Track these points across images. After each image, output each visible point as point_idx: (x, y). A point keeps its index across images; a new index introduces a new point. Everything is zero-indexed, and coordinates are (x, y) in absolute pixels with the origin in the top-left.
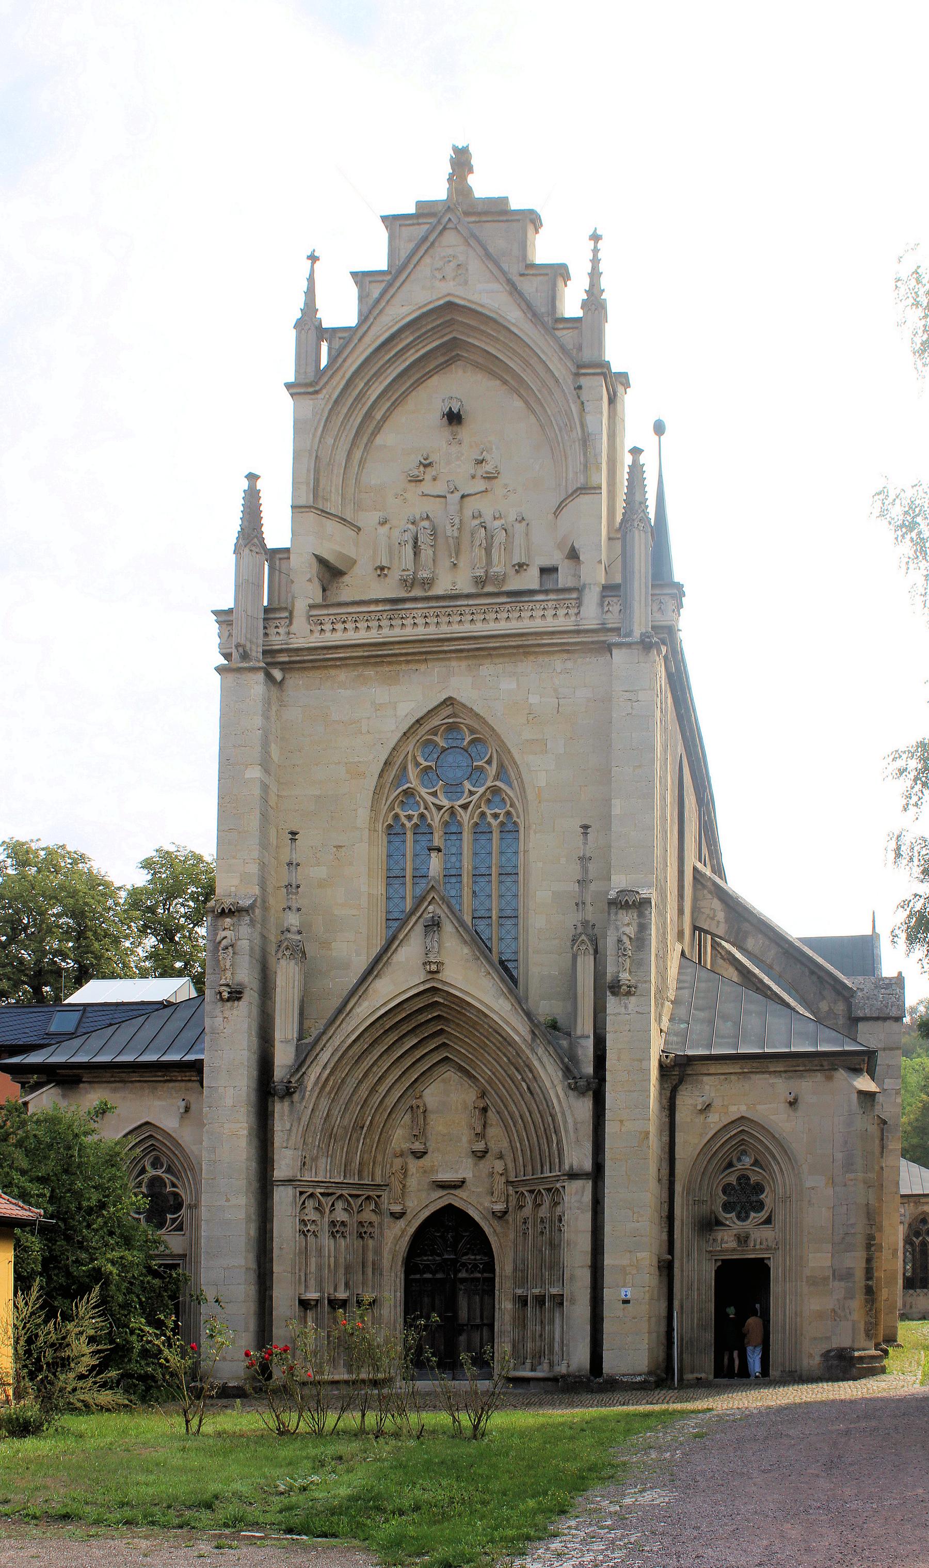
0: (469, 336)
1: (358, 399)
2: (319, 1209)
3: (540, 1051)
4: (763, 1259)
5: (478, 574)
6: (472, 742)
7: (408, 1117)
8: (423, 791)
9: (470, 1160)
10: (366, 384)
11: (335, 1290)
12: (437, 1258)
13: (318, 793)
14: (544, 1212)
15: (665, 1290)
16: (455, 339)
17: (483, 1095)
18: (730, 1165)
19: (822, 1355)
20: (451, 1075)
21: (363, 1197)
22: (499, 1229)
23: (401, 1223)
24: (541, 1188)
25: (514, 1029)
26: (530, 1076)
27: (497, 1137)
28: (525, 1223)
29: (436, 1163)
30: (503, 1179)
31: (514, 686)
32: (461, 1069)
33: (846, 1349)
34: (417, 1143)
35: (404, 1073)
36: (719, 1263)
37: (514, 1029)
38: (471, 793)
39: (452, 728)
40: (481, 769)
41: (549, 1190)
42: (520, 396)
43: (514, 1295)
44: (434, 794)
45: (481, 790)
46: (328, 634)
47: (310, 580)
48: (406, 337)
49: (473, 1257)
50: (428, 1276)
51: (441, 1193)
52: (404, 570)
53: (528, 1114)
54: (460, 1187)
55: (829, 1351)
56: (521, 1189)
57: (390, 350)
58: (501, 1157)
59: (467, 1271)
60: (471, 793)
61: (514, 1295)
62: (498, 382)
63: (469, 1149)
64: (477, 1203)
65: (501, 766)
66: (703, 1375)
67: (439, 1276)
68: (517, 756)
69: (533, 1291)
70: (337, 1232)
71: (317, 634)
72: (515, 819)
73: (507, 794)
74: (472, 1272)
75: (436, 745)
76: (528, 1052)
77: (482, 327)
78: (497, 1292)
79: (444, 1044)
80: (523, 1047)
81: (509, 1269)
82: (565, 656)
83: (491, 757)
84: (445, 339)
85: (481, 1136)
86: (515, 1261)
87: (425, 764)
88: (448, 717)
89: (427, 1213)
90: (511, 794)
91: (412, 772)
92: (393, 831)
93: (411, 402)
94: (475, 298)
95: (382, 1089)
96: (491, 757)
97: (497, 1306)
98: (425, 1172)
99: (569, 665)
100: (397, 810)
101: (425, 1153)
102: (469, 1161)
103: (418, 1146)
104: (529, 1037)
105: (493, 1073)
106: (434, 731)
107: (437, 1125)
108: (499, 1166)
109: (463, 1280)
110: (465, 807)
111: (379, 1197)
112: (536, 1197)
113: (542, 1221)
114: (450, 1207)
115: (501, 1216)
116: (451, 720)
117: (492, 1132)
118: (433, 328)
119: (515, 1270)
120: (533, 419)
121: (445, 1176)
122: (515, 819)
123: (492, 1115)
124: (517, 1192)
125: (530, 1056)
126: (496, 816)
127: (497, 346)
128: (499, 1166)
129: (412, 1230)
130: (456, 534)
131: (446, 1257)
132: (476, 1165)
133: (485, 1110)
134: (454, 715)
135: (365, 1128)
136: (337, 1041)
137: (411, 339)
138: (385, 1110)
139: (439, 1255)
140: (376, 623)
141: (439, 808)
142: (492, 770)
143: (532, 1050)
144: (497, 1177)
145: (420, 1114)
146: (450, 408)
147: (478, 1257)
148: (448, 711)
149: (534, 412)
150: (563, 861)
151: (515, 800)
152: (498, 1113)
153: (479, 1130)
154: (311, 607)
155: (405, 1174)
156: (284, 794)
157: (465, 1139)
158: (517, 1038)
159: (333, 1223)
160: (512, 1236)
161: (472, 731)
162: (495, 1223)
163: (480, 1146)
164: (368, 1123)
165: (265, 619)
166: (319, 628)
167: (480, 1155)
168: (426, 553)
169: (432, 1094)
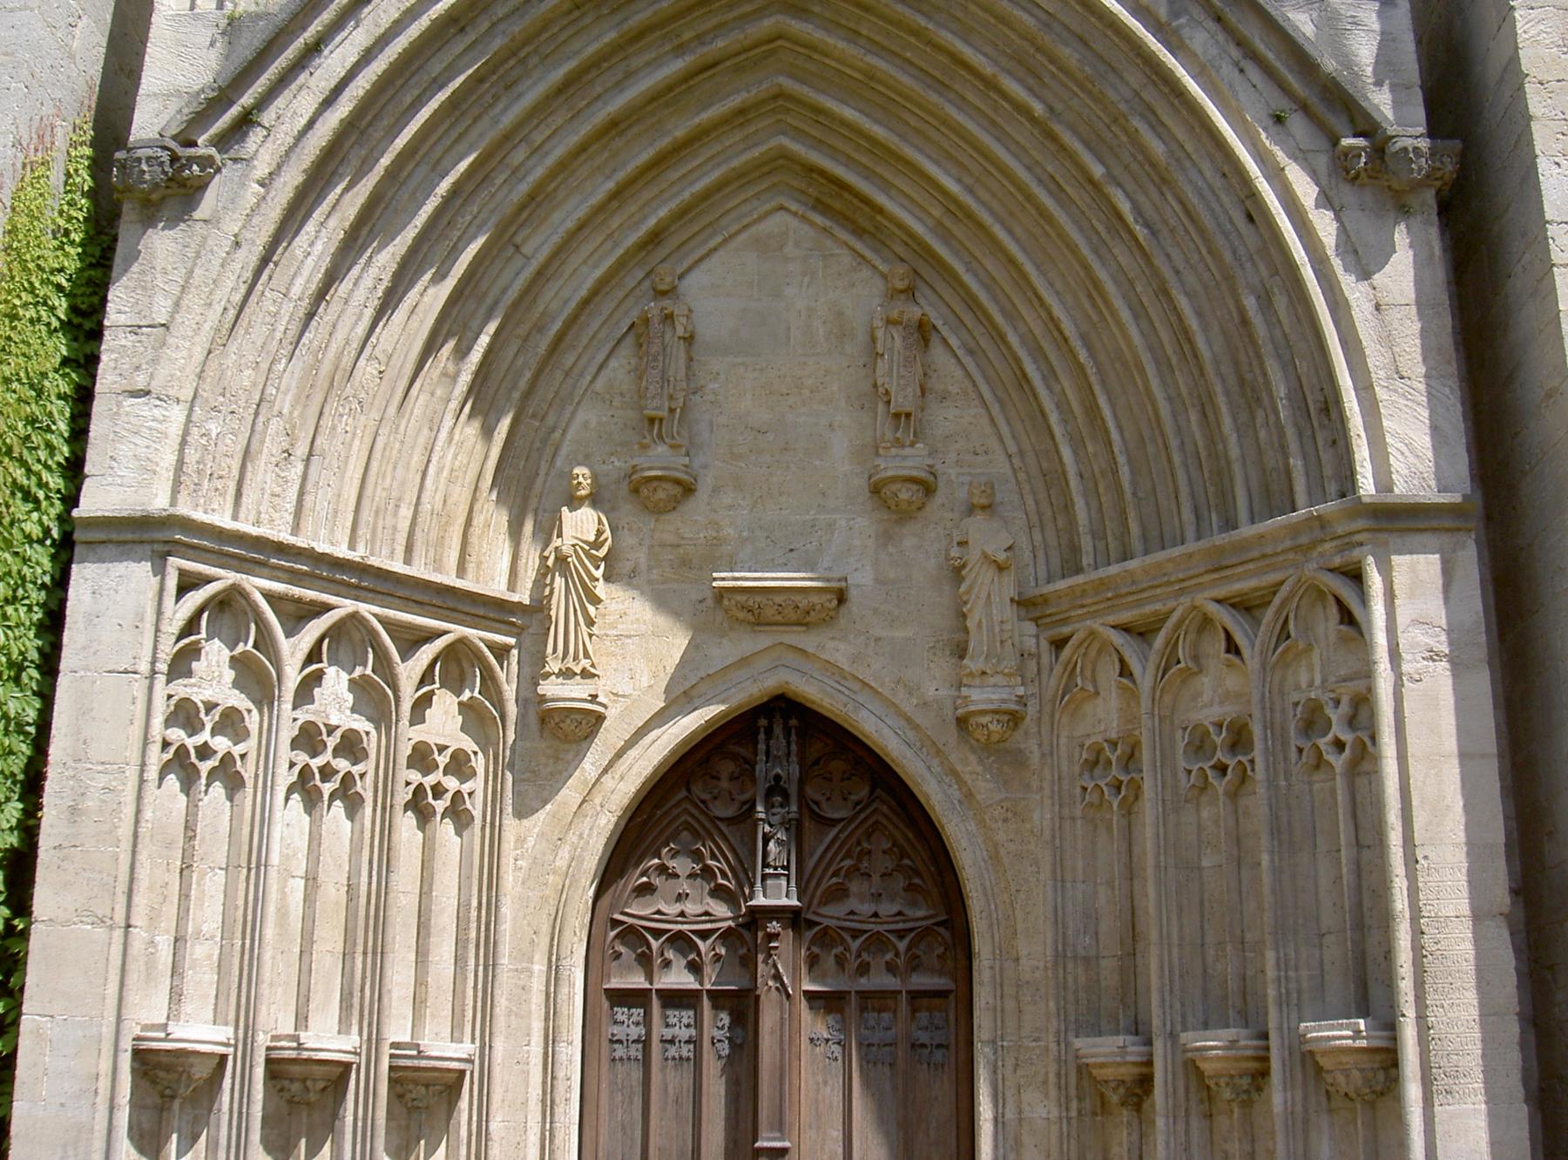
2: (255, 678)
7: (620, 368)
9: (862, 522)
11: (302, 1019)
20: (788, 224)
21: (440, 644)
22: (984, 788)
27: (966, 434)
29: (729, 531)
30: (1007, 588)
34: (661, 449)
35: (616, 195)
49: (866, 908)
51: (749, 643)
54: (828, 620)
56: (1095, 624)
59: (840, 962)
63: (860, 483)
70: (327, 772)
74: (864, 969)
79: (780, 95)
81: (1034, 952)
86: (1058, 921)
95: (539, 244)
98: (685, 562)
101: (688, 490)
107: (734, 396)
108: (987, 538)
111: (501, 652)
115: (996, 740)
117: (947, 418)
119: (1060, 957)
131: (760, 900)
132: (886, 538)
138: (540, 328)
144: (981, 580)
147: (887, 908)
153: (904, 399)
157: (840, 445)
159: (308, 738)
160: (1042, 816)
162: (970, 766)
167: (898, 500)
169: (715, 291)
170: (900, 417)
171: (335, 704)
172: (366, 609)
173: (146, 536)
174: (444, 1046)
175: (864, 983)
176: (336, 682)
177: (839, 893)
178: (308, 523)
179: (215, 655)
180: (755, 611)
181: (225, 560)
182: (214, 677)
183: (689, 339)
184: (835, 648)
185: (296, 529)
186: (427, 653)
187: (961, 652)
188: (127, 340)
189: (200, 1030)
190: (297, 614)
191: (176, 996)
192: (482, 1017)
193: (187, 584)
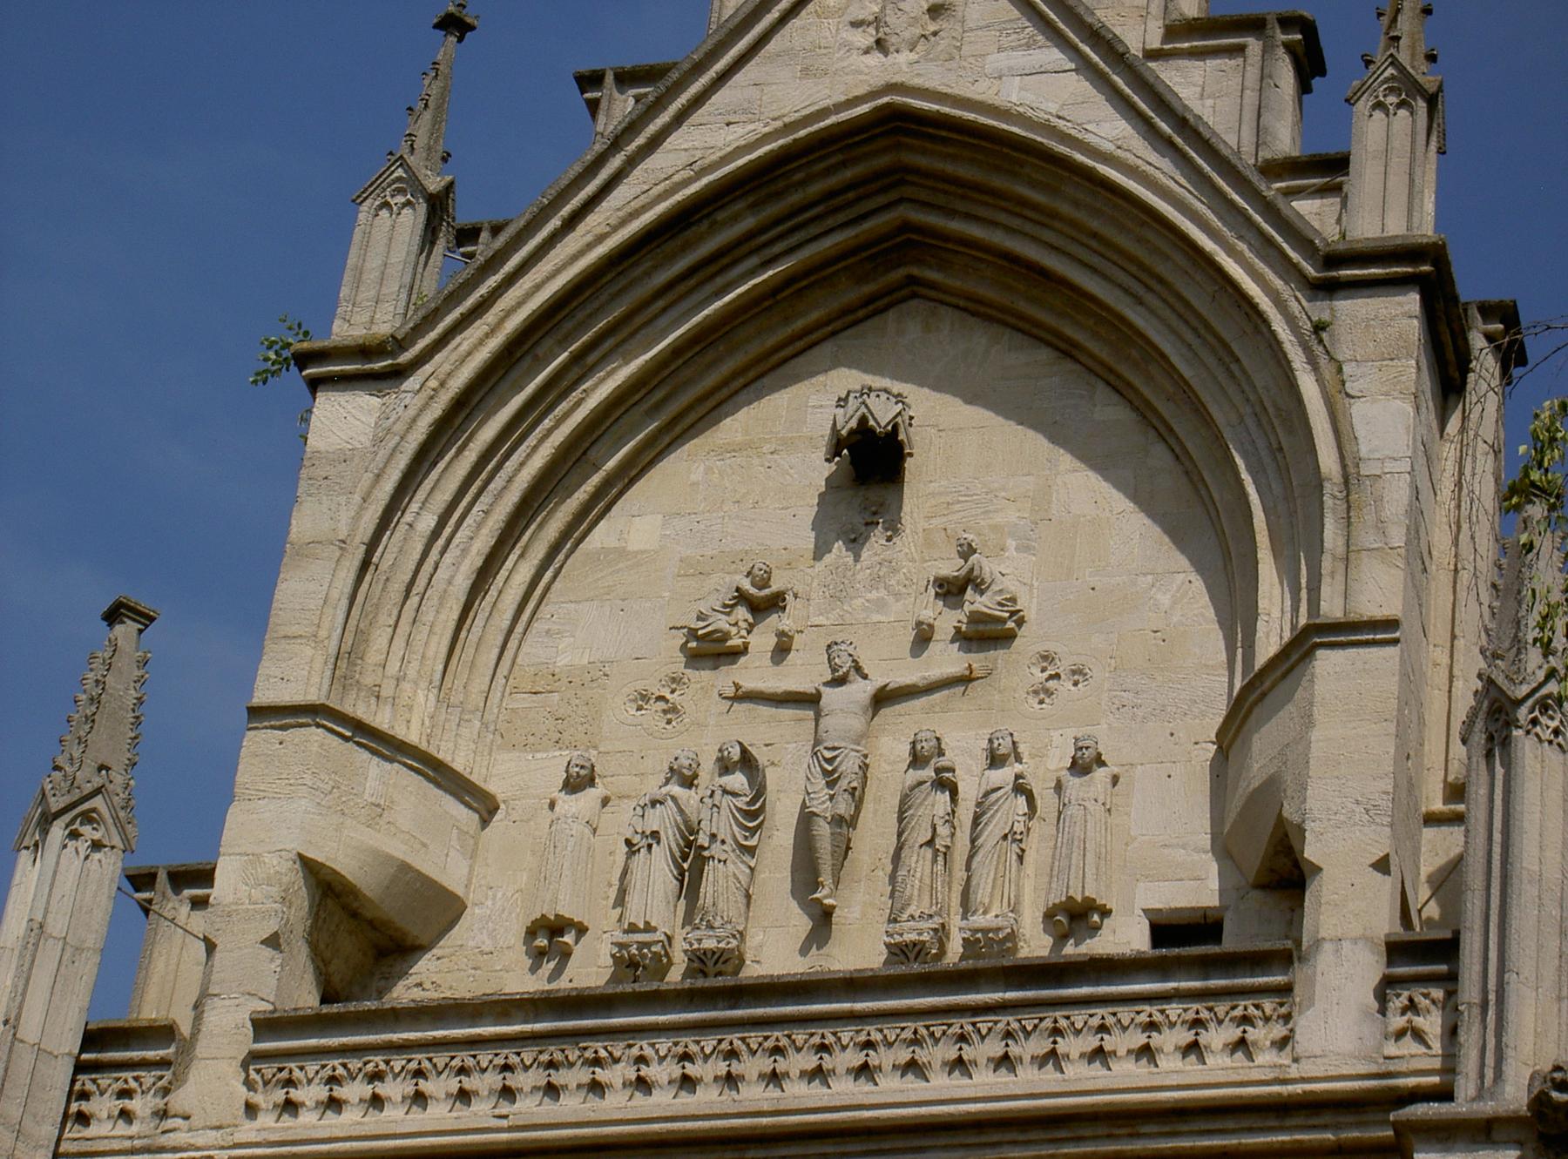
0: (952, 213)
5: (911, 937)
10: (576, 358)
16: (906, 227)
42: (1121, 389)
46: (307, 1118)
47: (273, 942)
48: (735, 219)
52: (633, 929)
57: (671, 258)
62: (1044, 354)
71: (266, 1120)
77: (998, 182)
93: (735, 426)
94: (982, 91)
118: (831, 194)
120: (1160, 456)
127: (1047, 235)
130: (844, 807)
137: (749, 223)
140: (493, 1080)
146: (863, 420)
149: (1163, 432)
154: (264, 1026)
165: (81, 1068)
166: (279, 1095)
168: (720, 881)
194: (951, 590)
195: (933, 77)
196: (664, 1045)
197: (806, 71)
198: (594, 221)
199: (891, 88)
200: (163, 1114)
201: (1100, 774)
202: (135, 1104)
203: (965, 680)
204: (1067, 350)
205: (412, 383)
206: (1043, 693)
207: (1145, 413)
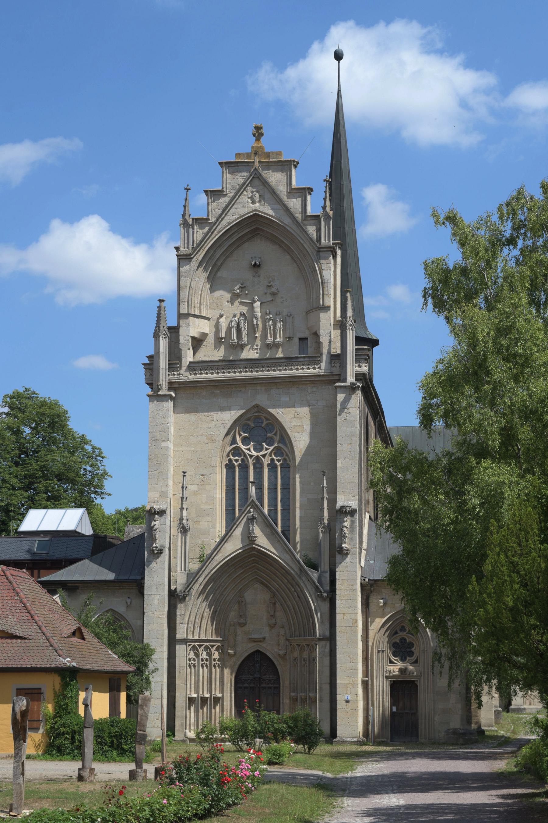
1: (210, 258)
3: (304, 578)
4: (414, 681)
6: (267, 424)
7: (236, 607)
8: (243, 447)
11: (203, 692)
12: (251, 677)
13: (193, 449)
14: (305, 655)
15: (365, 695)
17: (274, 596)
18: (396, 633)
19: (445, 732)
20: (258, 585)
23: (234, 659)
24: (304, 644)
25: (291, 568)
26: (299, 589)
28: (295, 660)
30: (285, 638)
31: (287, 399)
32: (262, 583)
33: (457, 729)
36: (392, 682)
37: (291, 568)
38: (267, 449)
39: (257, 418)
40: (271, 438)
41: (308, 645)
43: (290, 696)
44: (249, 449)
45: (272, 448)
50: (246, 685)
51: (253, 644)
53: (297, 607)
55: (449, 730)
58: (283, 627)
60: (267, 449)
61: (290, 696)
64: (271, 649)
65: (281, 436)
66: (385, 740)
67: (252, 685)
68: (289, 433)
69: (301, 694)
70: (204, 663)
72: (288, 462)
73: (284, 450)
74: (268, 684)
75: (249, 425)
76: (298, 579)
78: (281, 695)
80: (296, 576)
81: (287, 683)
82: (313, 385)
83: (276, 432)
84: (252, 228)
85: (273, 616)
87: (244, 435)
88: (256, 412)
89: (247, 654)
90: (286, 450)
91: (238, 439)
92: (230, 467)
96: (276, 432)
97: (281, 701)
99: (315, 389)
100: (231, 457)
101: (245, 624)
102: (267, 629)
103: (242, 621)
104: (298, 572)
105: (280, 586)
106: (249, 419)
108: (282, 632)
109: (265, 688)
110: (264, 456)
112: (301, 648)
113: (304, 660)
114: (258, 651)
115: (283, 657)
116: (257, 414)
121: (256, 636)
122: (288, 462)
123: (278, 605)
124: (291, 645)
125: (299, 581)
126: (278, 460)
128: (282, 632)
129: (239, 663)
131: (256, 676)
133: (275, 604)
134: (259, 412)
135: (217, 613)
136: (206, 572)
139: (251, 675)
141: (251, 456)
142: (277, 438)
143: (300, 578)
145: (242, 604)
147: (271, 676)
148: (256, 409)
150: (312, 484)
151: (288, 453)
152: (281, 605)
153: (272, 613)
155: (236, 635)
156: (176, 449)
158: (293, 572)
161: (267, 419)
163: (272, 622)
164: (218, 610)
167: (272, 626)
170: (271, 616)
171: (204, 655)
172: (208, 644)
173: (185, 641)
174: (219, 695)
175: (268, 686)
176: (205, 653)
177: (265, 675)
178: (201, 635)
179: (192, 653)
180: (255, 641)
181: (193, 642)
182: (192, 655)
183: (245, 604)
184: (264, 645)
185: (199, 637)
186: (215, 647)
187: (279, 645)
188: (179, 617)
189: (194, 695)
190: (200, 646)
191: (190, 691)
192: (222, 691)
193: (189, 645)
194: (269, 286)
195: (262, 208)
196: (243, 366)
197: (243, 207)
198: (216, 232)
199: (256, 210)
200: (179, 374)
201: (291, 317)
202: (175, 373)
203: (272, 300)
204: (281, 247)
205: (193, 260)
206: (282, 303)
207: (293, 258)
